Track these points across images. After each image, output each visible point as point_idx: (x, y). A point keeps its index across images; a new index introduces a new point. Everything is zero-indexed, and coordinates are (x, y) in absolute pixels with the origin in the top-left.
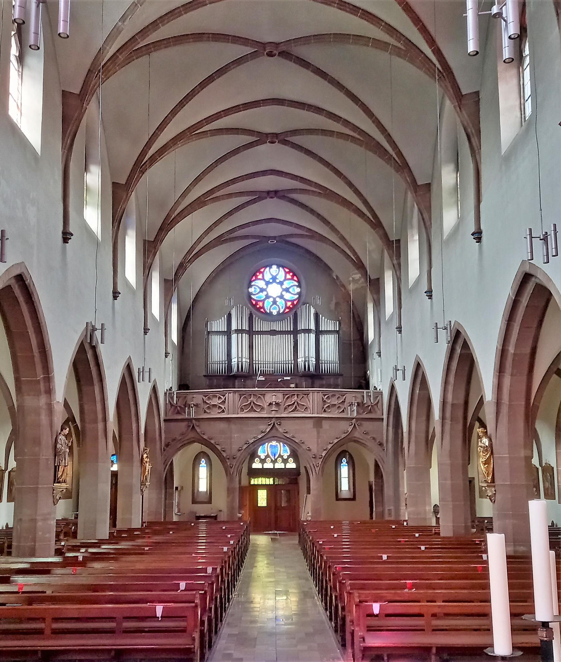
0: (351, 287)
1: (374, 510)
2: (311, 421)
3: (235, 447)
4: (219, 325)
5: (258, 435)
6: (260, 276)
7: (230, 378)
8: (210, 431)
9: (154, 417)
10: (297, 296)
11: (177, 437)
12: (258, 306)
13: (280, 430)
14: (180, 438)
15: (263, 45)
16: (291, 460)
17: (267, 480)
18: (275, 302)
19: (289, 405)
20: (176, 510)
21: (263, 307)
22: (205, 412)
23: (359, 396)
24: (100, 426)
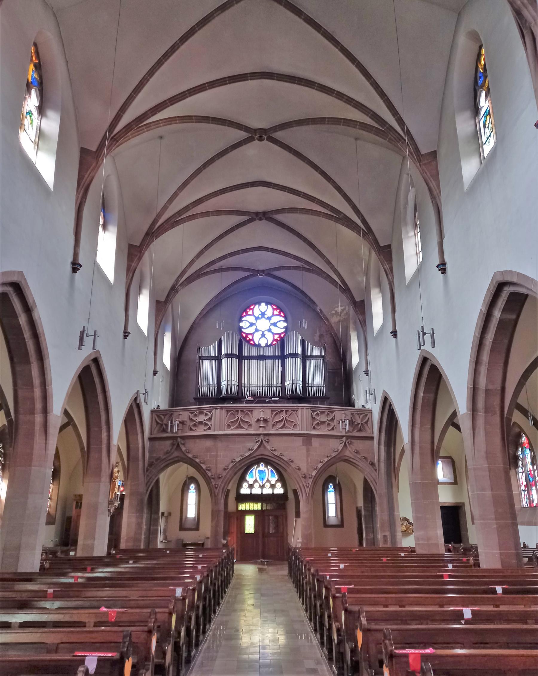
0: (334, 320)
1: (364, 537)
2: (300, 439)
3: (221, 466)
4: (210, 350)
5: (246, 452)
6: (250, 312)
7: (220, 398)
8: (195, 448)
9: (137, 434)
10: (284, 330)
11: (161, 456)
12: (248, 339)
13: (269, 447)
14: (165, 457)
15: (255, 131)
16: (279, 485)
17: (255, 505)
18: (263, 335)
19: (277, 422)
20: (160, 537)
21: (252, 340)
22: (191, 429)
23: (349, 413)
24: (39, 418)
